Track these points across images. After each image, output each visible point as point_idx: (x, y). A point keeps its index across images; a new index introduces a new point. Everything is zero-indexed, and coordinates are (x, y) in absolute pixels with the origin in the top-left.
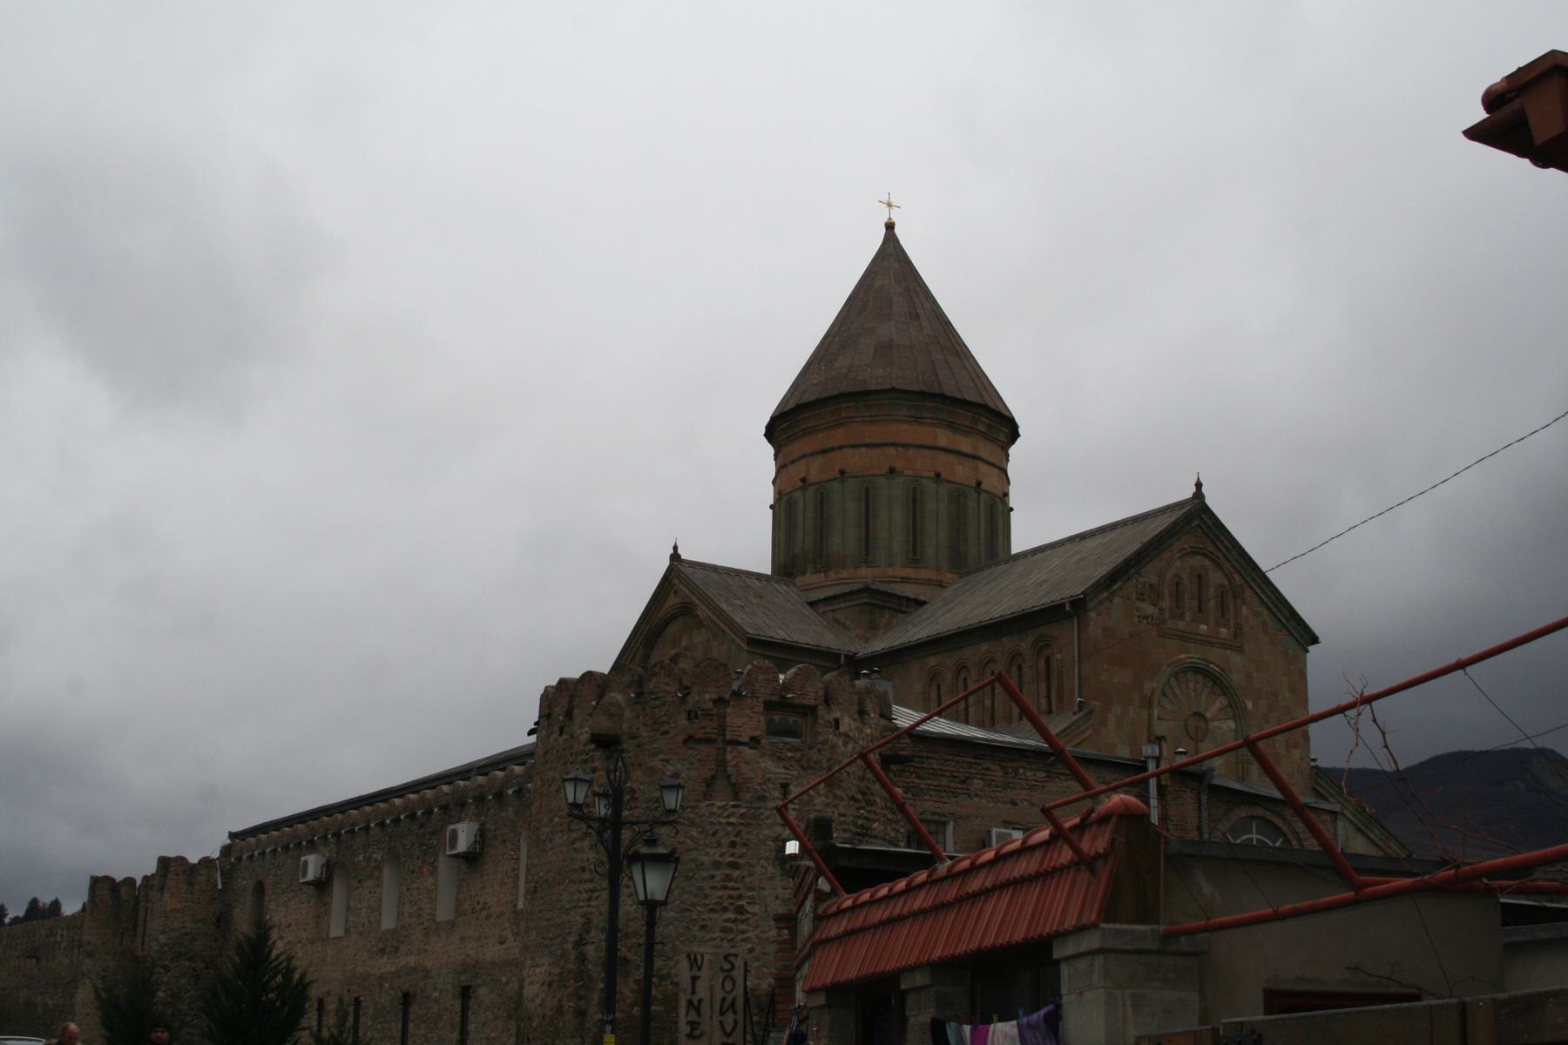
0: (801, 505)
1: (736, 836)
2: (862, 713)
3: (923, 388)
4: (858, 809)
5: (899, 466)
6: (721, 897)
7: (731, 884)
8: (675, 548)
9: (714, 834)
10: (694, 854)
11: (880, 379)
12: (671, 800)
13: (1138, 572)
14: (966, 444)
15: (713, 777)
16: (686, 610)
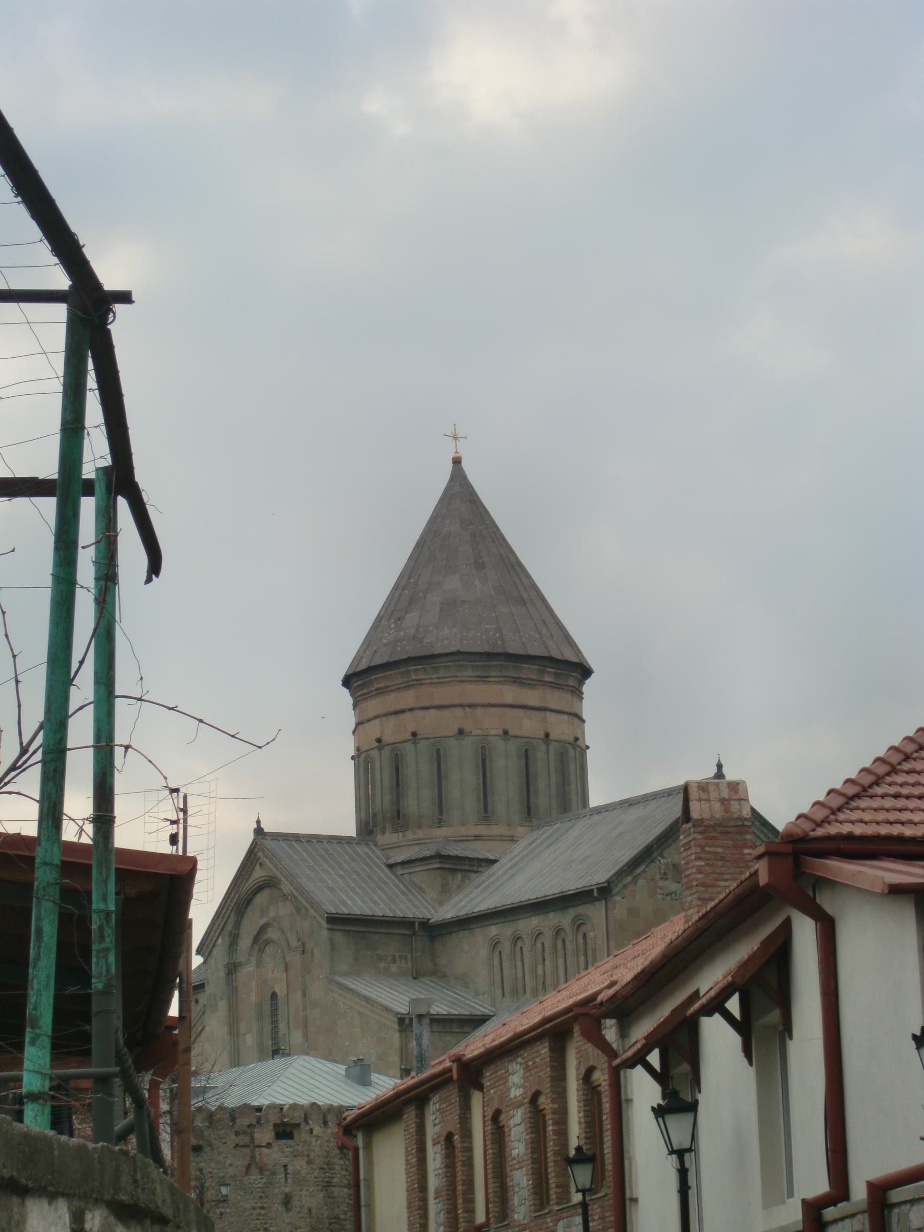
0: (377, 765)
1: (263, 1193)
2: (325, 1123)
3: (486, 648)
4: (325, 1173)
5: (467, 727)
6: (256, 1224)
7: (261, 1217)
8: (258, 822)
9: (251, 1193)
10: (241, 1203)
11: (446, 641)
12: (224, 1190)
13: (661, 855)
14: (532, 697)
15: (249, 1164)
16: (270, 883)
